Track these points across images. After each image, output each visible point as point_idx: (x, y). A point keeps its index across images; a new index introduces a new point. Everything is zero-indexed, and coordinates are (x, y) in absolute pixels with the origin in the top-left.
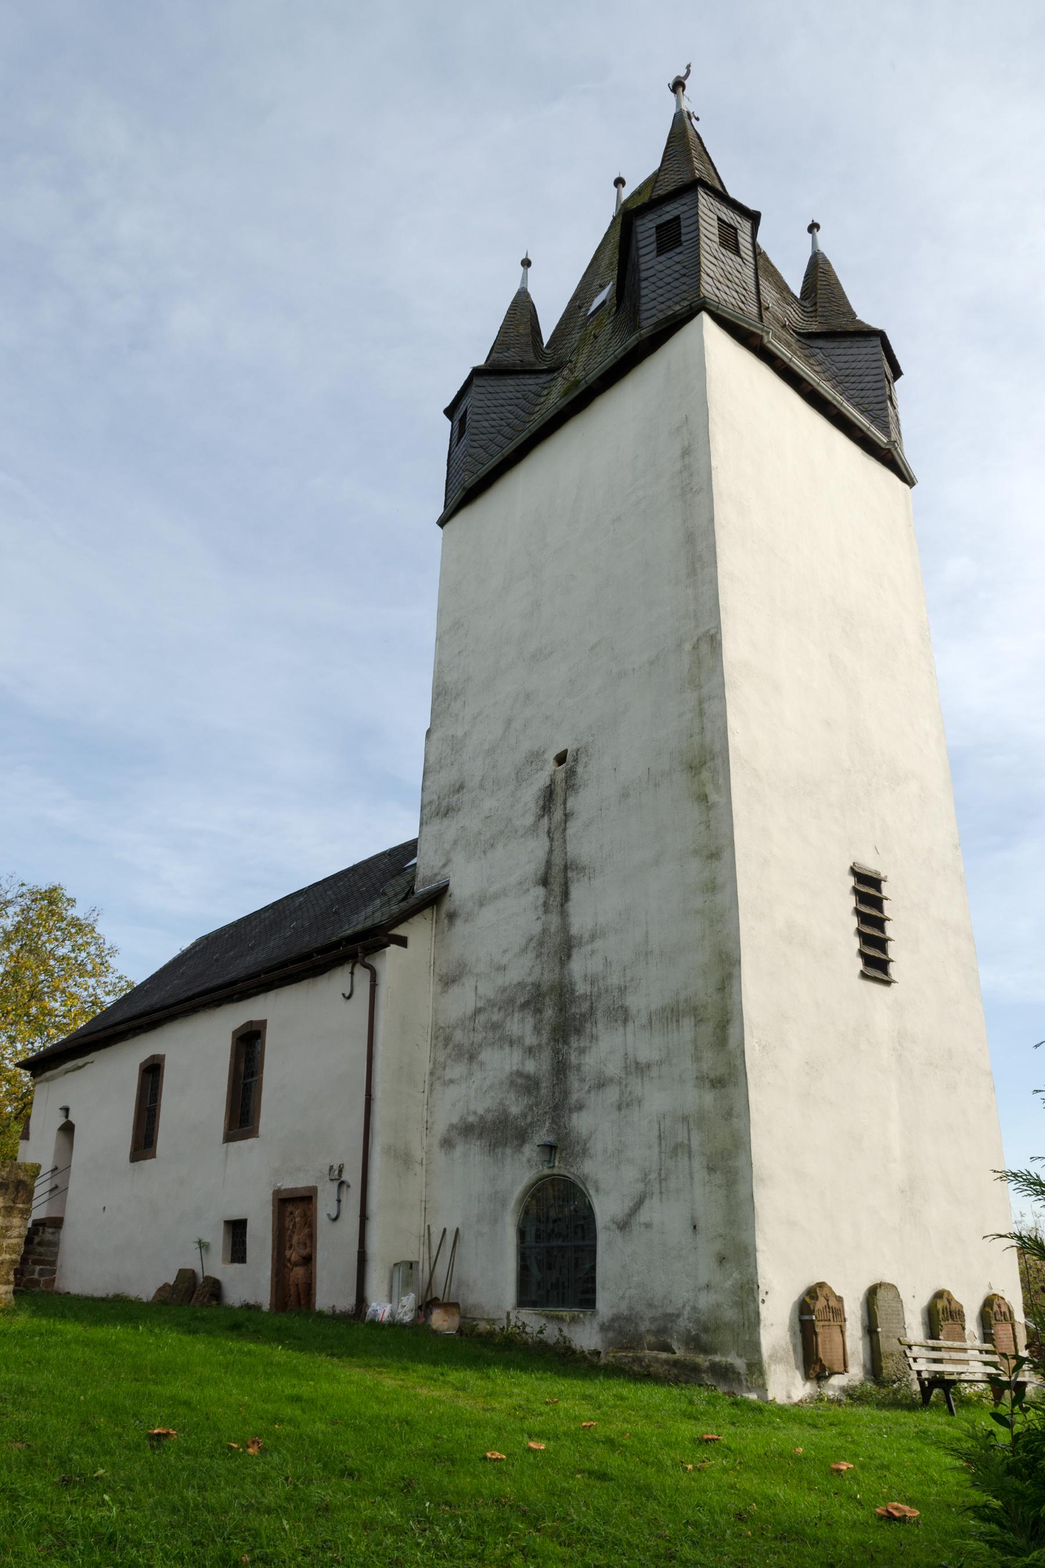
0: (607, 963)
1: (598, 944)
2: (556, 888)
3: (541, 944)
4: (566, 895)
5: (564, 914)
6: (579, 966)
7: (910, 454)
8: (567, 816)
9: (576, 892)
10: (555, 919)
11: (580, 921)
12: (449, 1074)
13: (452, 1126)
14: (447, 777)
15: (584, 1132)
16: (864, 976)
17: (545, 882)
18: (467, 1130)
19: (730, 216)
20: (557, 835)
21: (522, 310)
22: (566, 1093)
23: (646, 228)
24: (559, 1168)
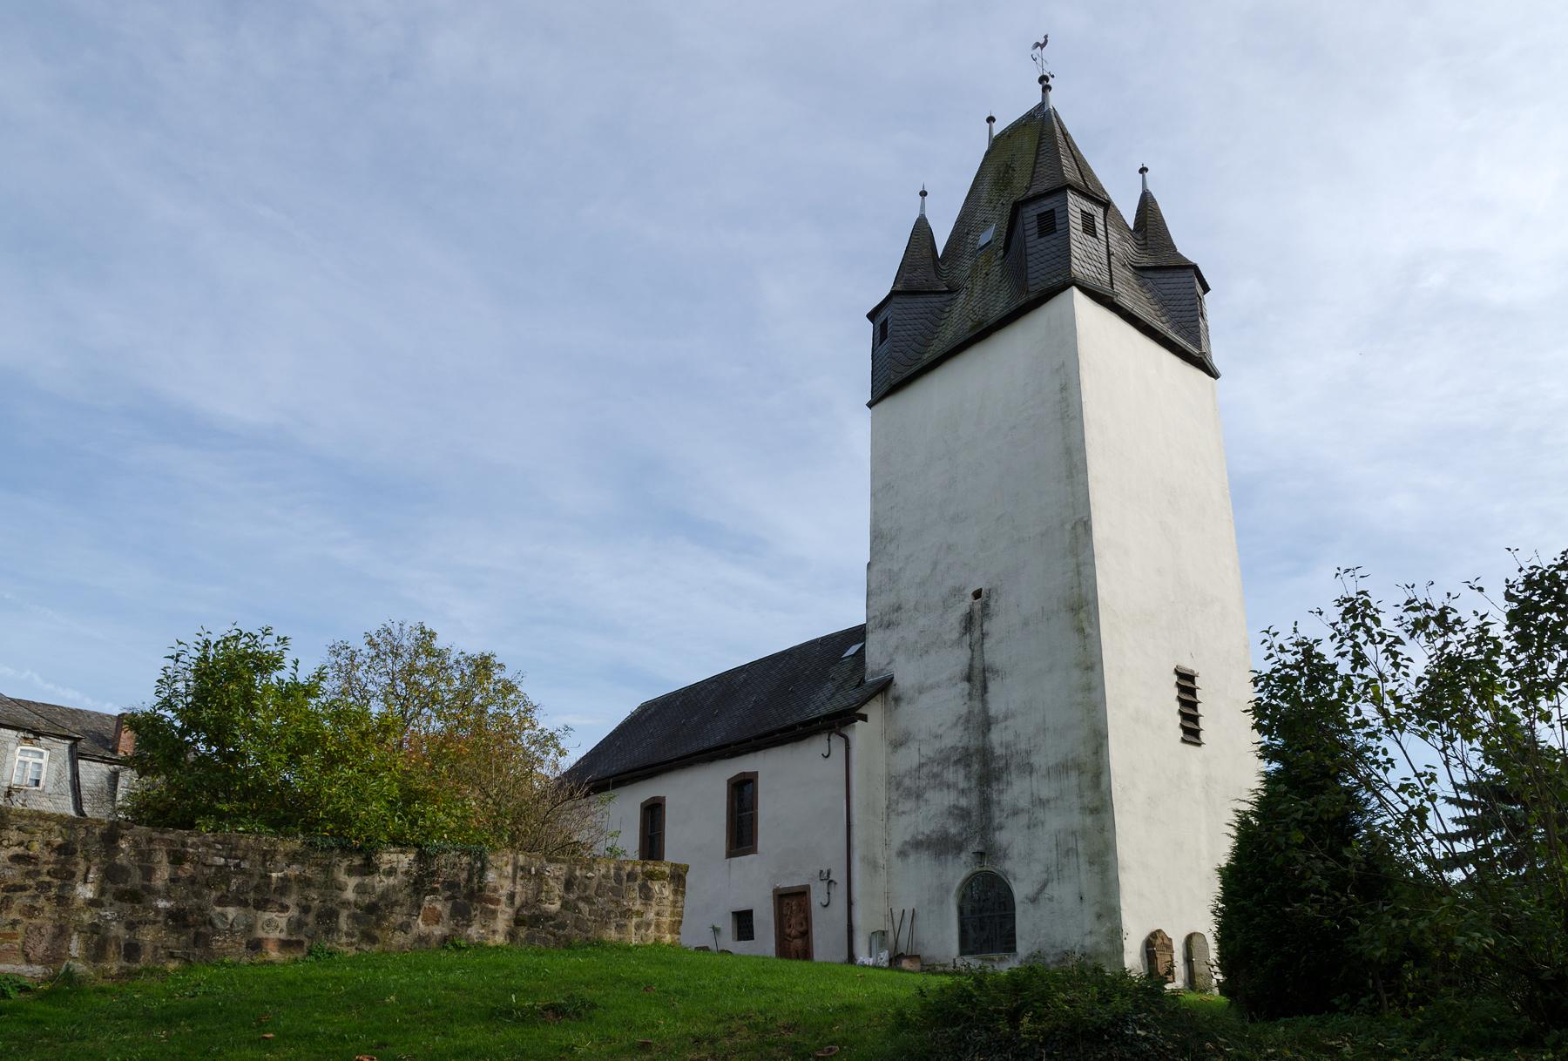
0: (1017, 735)
1: (1010, 722)
2: (978, 684)
3: (968, 721)
4: (985, 689)
5: (984, 701)
6: (996, 737)
8: (983, 635)
10: (977, 706)
11: (996, 706)
12: (901, 808)
13: (906, 843)
14: (886, 600)
15: (1005, 844)
16: (1184, 741)
17: (969, 679)
18: (917, 845)
19: (1088, 206)
20: (977, 646)
21: (922, 231)
22: (990, 819)
23: (1031, 214)
24: (987, 867)
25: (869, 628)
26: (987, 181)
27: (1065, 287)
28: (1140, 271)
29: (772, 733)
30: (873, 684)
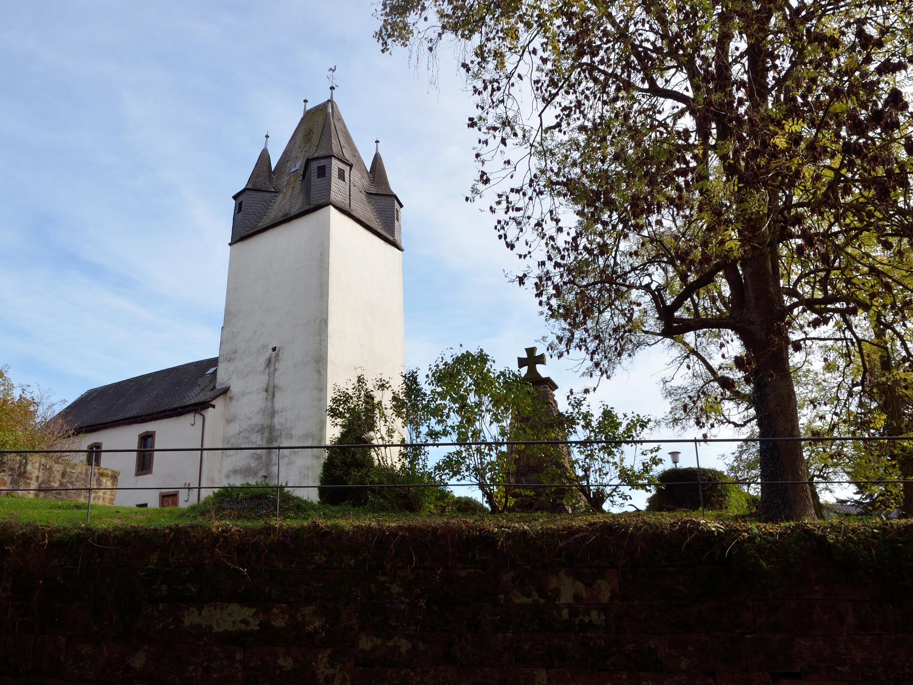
0: (286, 420)
1: (284, 413)
2: (271, 393)
4: (274, 396)
5: (272, 402)
6: (277, 420)
7: (403, 246)
8: (275, 370)
9: (277, 395)
10: (269, 404)
11: (278, 405)
17: (267, 391)
18: (235, 472)
21: (264, 157)
22: (271, 460)
25: (220, 360)
26: (301, 134)
27: (327, 205)
28: (369, 194)
29: (165, 411)
30: (220, 389)
